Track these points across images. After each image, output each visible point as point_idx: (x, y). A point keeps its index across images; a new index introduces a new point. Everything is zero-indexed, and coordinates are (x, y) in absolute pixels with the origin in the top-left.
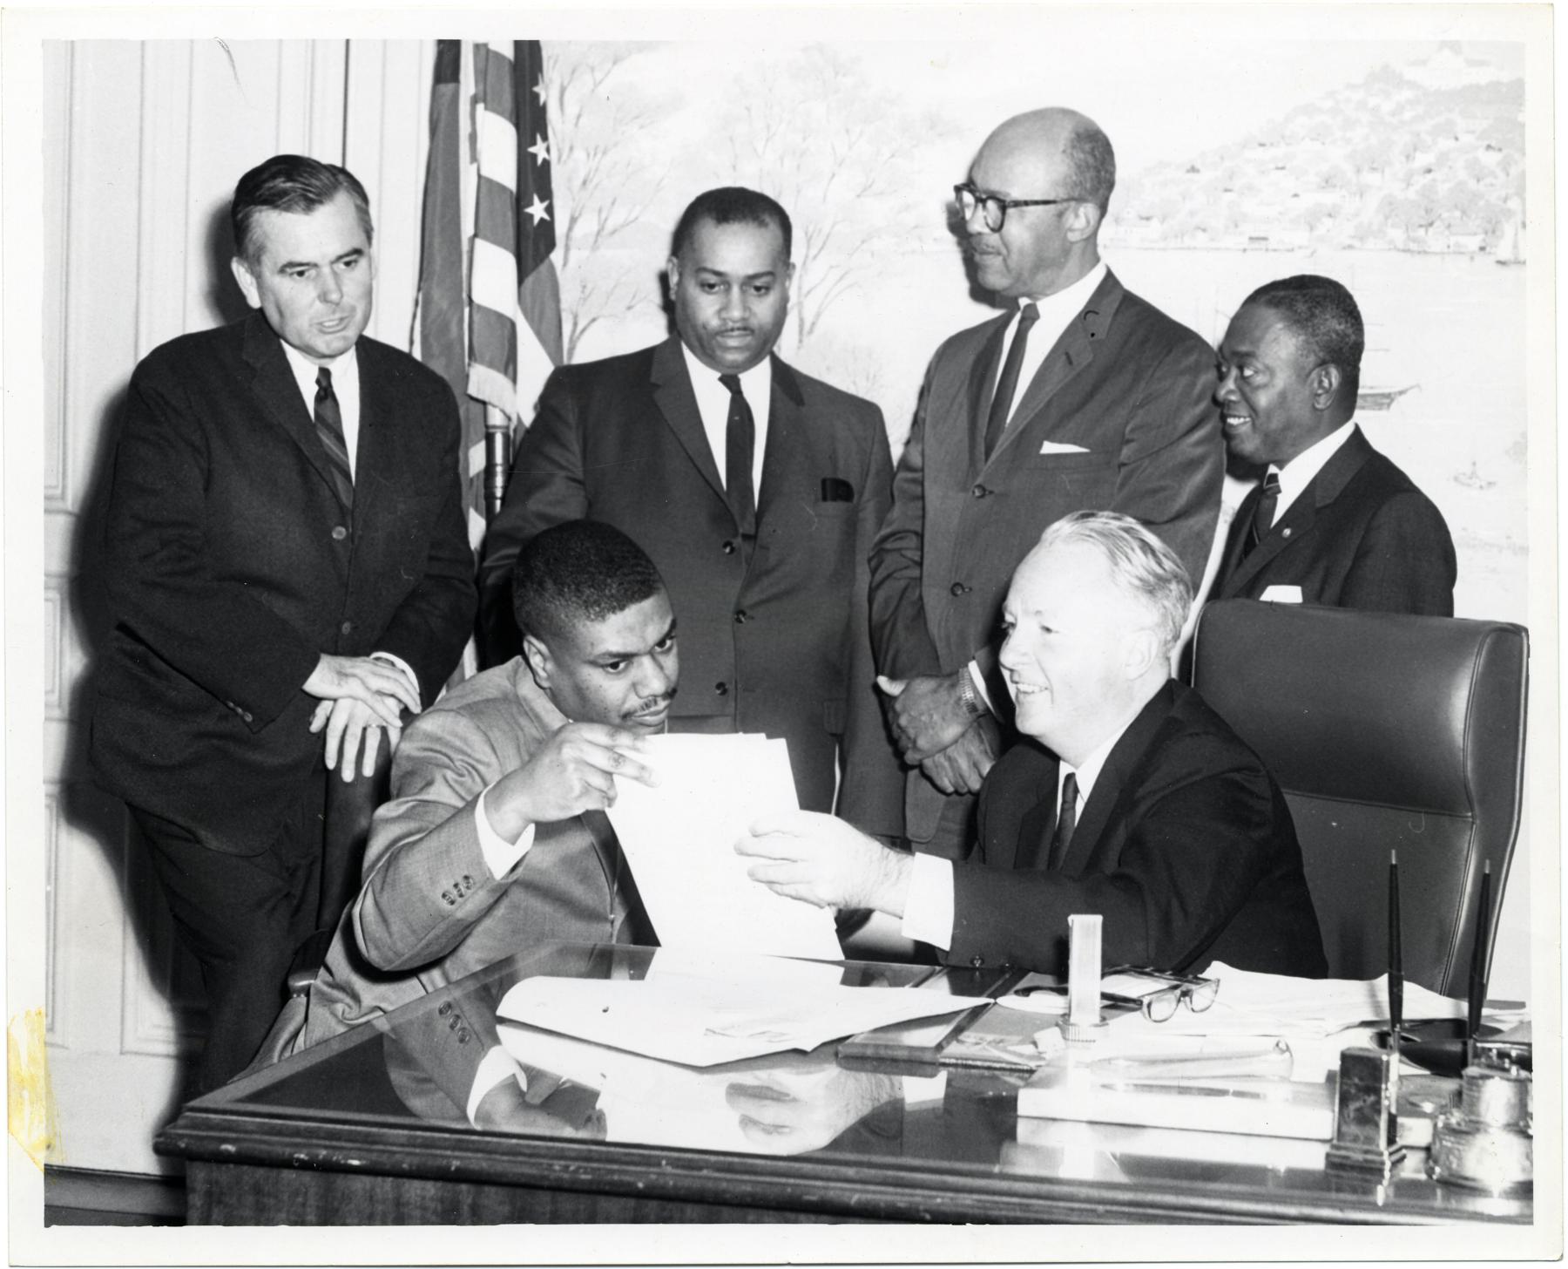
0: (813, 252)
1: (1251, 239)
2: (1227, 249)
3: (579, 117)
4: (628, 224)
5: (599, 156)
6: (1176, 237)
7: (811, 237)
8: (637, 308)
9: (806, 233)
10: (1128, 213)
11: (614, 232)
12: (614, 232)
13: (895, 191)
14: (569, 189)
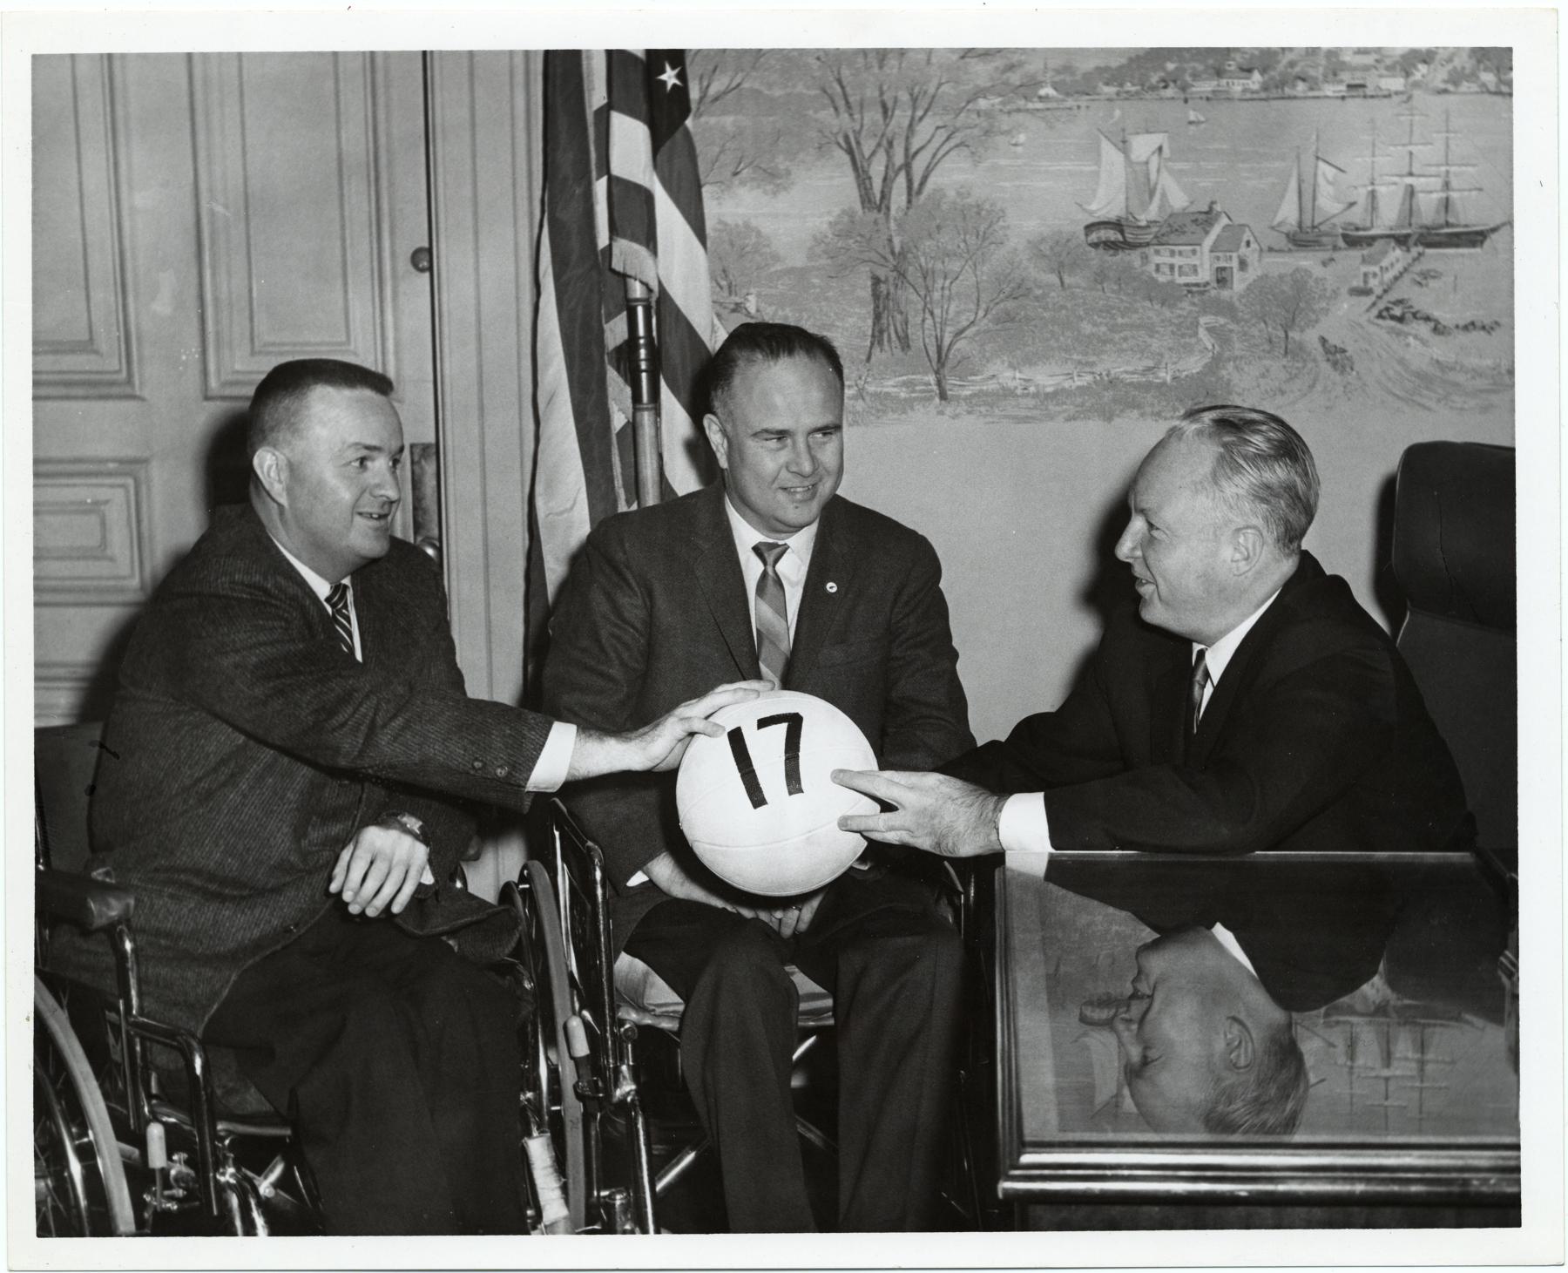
0: (920, 113)
1: (1350, 87)
6: (1277, 87)
7: (917, 96)
8: (745, 171)
9: (911, 95)
12: (716, 99)
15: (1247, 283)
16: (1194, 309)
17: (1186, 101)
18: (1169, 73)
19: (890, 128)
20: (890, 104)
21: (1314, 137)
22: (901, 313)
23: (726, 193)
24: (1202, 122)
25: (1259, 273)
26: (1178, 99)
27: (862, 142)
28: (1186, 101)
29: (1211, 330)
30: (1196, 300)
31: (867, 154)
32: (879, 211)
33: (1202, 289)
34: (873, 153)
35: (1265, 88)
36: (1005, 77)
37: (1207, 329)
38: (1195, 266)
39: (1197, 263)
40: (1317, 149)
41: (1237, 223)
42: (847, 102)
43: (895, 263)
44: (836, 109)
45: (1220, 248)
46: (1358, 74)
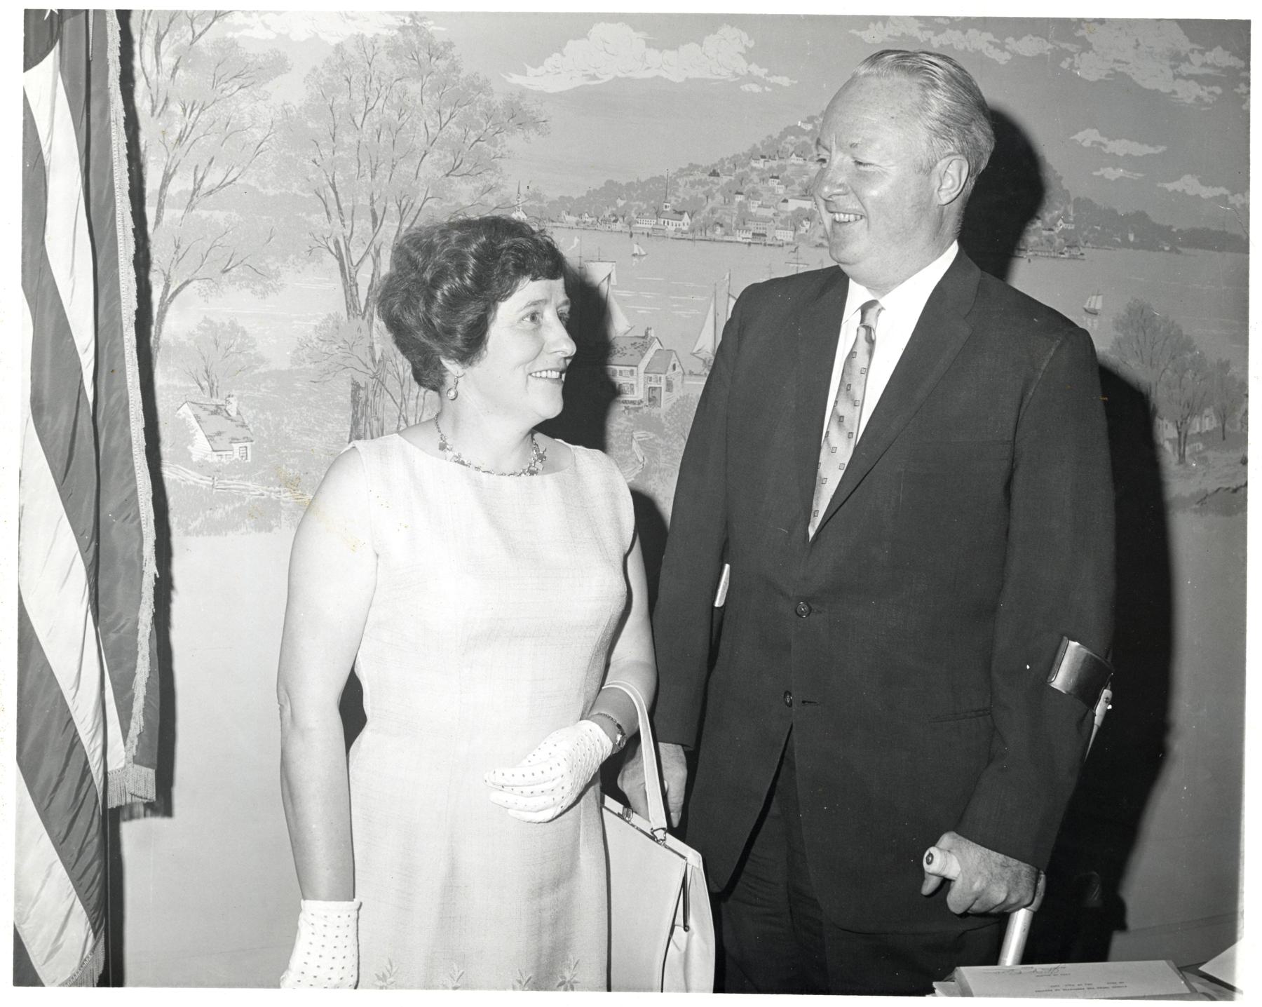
2: (737, 242)
3: (176, 68)
4: (224, 186)
5: (196, 112)
7: (405, 209)
9: (400, 207)
10: (666, 207)
11: (210, 193)
12: (210, 193)
13: (480, 173)
14: (164, 144)
15: (672, 402)
16: (628, 423)
17: (631, 236)
18: (617, 208)
19: (378, 236)
20: (379, 213)
21: (727, 277)
22: (378, 420)
23: (214, 290)
24: (644, 256)
25: (682, 395)
26: (626, 232)
27: (351, 248)
28: (631, 236)
29: (641, 444)
30: (631, 416)
31: (355, 264)
32: (363, 318)
33: (637, 406)
34: (361, 261)
35: (693, 231)
36: (482, 197)
37: (639, 443)
38: (632, 385)
39: (634, 382)
40: (729, 287)
41: (665, 349)
42: (340, 208)
43: (375, 371)
44: (328, 214)
45: (653, 371)
46: (762, 225)
